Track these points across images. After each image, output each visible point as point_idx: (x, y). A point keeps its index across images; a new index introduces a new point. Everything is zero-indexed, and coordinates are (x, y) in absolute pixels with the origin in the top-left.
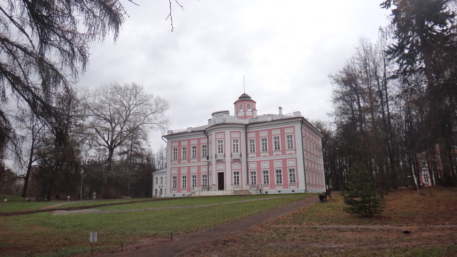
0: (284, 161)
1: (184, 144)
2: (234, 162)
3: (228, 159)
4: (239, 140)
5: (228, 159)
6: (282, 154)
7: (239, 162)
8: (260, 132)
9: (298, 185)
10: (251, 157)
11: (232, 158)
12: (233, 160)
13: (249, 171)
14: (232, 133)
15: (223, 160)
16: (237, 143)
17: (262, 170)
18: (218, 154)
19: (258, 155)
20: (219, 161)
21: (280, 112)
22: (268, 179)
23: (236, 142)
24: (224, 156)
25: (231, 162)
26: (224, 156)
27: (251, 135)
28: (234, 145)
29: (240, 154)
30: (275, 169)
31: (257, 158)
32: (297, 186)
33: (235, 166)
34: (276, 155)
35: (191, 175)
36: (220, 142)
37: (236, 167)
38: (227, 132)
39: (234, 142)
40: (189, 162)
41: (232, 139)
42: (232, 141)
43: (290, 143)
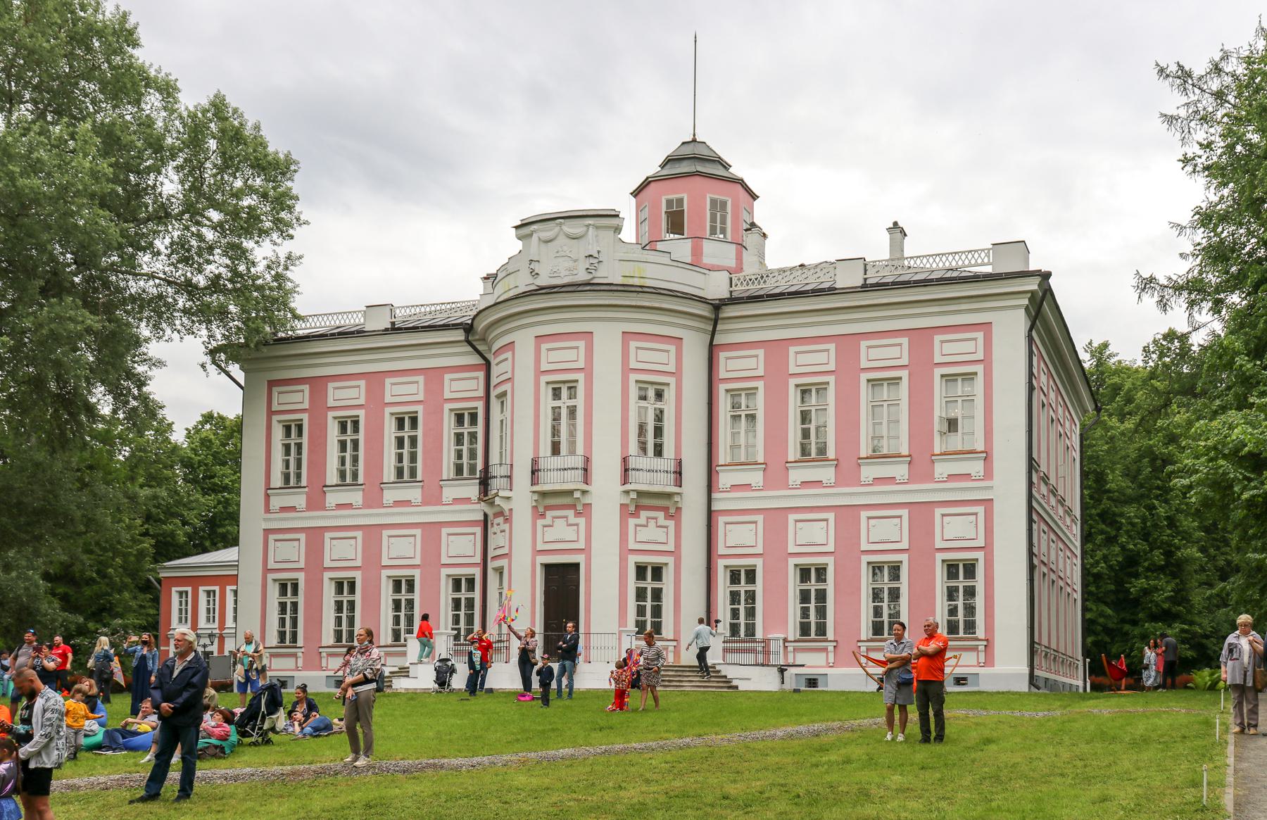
4: (673, 386)
7: (665, 509)
10: (735, 487)
11: (628, 487)
12: (633, 495)
13: (721, 563)
15: (577, 495)
18: (548, 462)
19: (775, 472)
23: (651, 393)
24: (580, 472)
26: (586, 470)
33: (644, 534)
34: (878, 480)
36: (565, 393)
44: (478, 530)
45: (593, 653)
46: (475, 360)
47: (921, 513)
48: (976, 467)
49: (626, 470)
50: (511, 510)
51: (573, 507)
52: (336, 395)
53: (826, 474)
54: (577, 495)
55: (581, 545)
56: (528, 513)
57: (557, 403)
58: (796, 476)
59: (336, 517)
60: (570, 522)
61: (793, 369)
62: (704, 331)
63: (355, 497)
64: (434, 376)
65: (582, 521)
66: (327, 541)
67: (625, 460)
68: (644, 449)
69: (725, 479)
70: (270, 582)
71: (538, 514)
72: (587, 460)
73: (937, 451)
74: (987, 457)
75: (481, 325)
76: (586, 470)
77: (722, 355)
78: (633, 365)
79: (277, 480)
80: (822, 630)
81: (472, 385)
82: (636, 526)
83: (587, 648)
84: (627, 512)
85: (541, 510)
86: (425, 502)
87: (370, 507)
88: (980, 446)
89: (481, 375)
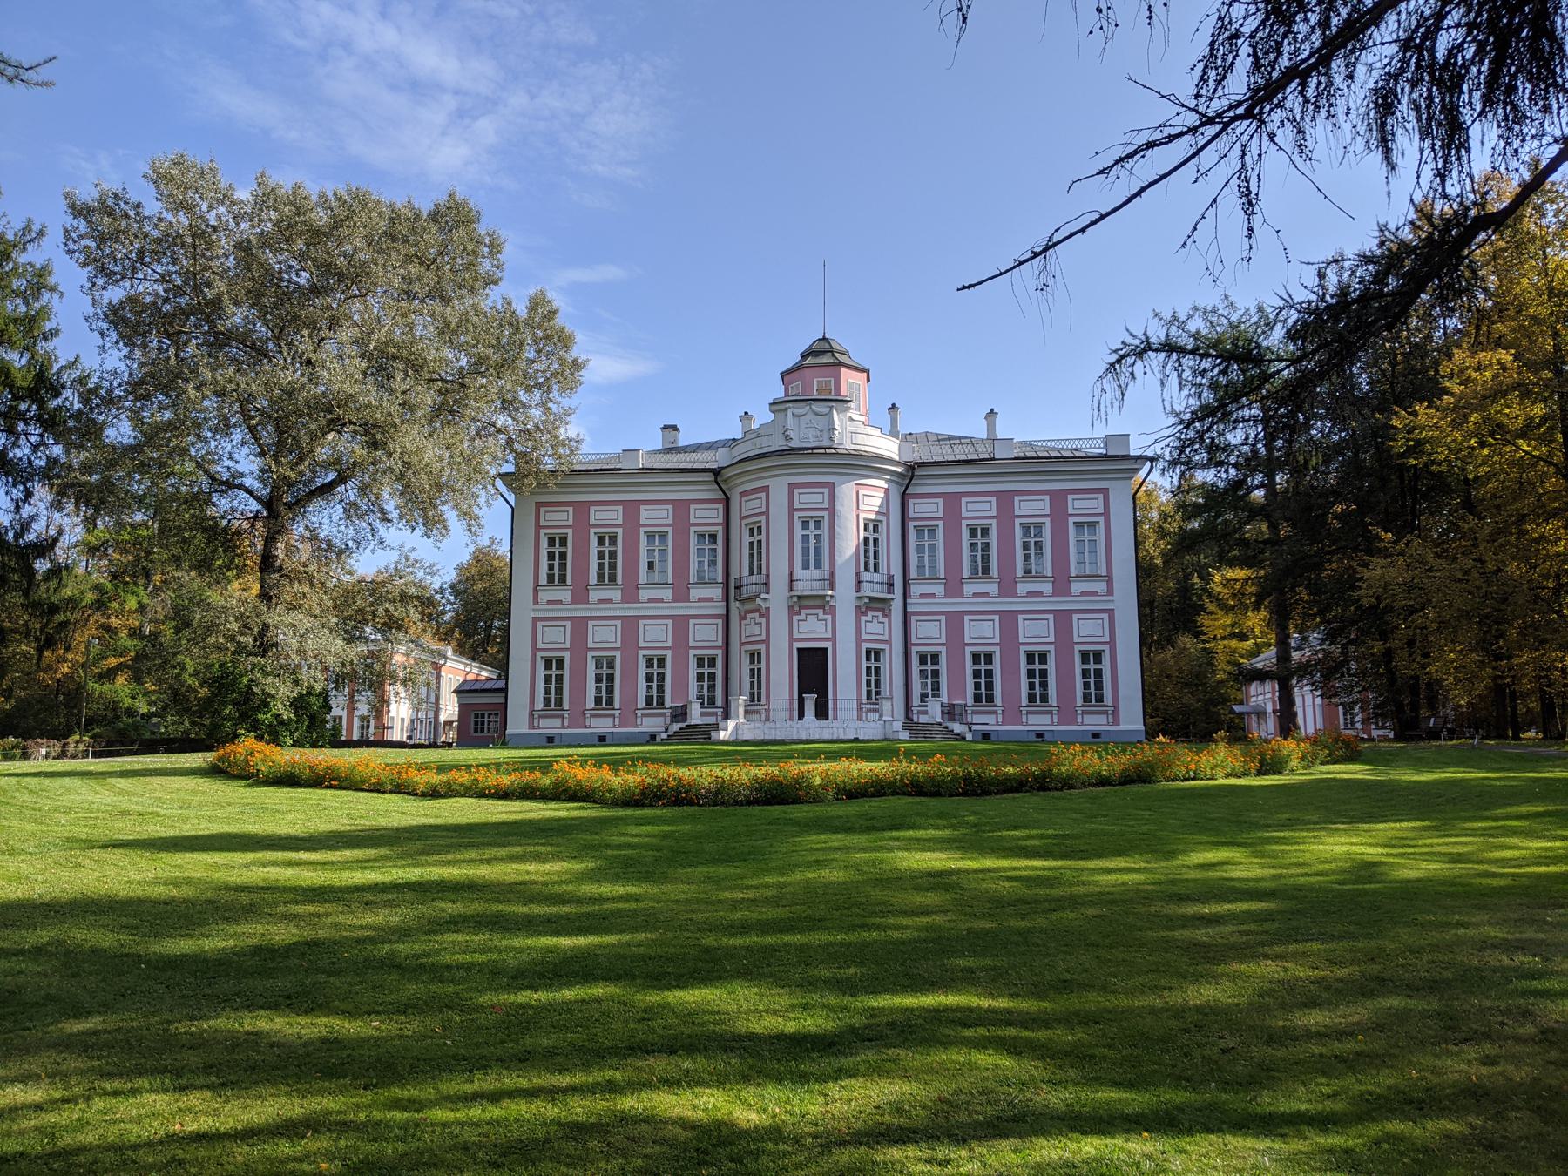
0: (1063, 620)
1: (607, 518)
2: (868, 608)
5: (845, 597)
6: (1003, 593)
8: (964, 500)
9: (1115, 707)
10: (922, 596)
13: (914, 650)
15: (828, 599)
16: (876, 536)
17: (968, 649)
18: (800, 574)
20: (801, 603)
21: (991, 427)
22: (990, 686)
25: (858, 608)
27: (926, 509)
30: (1077, 648)
32: (1111, 717)
35: (641, 653)
36: (812, 525)
37: (875, 627)
38: (779, 487)
40: (1008, 588)
43: (606, 562)
44: (720, 622)
45: (839, 713)
46: (720, 495)
50: (767, 609)
51: (823, 607)
52: (597, 516)
53: (993, 588)
54: (828, 599)
57: (806, 532)
58: (1023, 588)
62: (901, 485)
63: (615, 594)
64: (681, 507)
65: (829, 617)
66: (590, 627)
67: (858, 574)
69: (916, 589)
70: (538, 658)
72: (832, 574)
74: (1109, 579)
75: (727, 473)
77: (911, 502)
79: (543, 580)
80: (990, 698)
81: (714, 514)
83: (835, 709)
84: (860, 612)
85: (797, 608)
89: (721, 507)
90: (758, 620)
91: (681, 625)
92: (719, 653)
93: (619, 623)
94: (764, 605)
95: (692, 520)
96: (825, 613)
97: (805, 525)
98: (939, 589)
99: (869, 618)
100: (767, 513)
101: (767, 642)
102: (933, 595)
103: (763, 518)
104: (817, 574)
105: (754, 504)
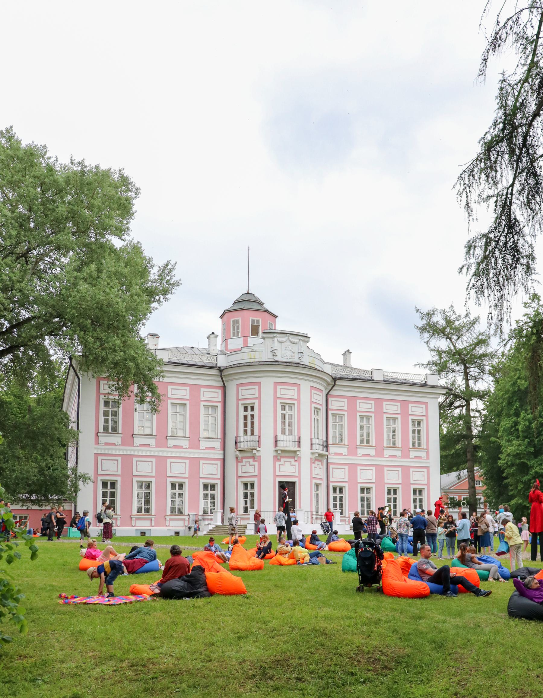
3: (305, 452)
14: (279, 387)
26: (258, 441)
28: (245, 417)
29: (257, 439)
31: (347, 457)
39: (246, 409)
41: (279, 401)
42: (279, 407)
47: (406, 470)
48: (423, 454)
49: (276, 441)
53: (372, 452)
55: (256, 474)
56: (272, 459)
59: (140, 450)
60: (251, 464)
61: (358, 409)
68: (246, 432)
71: (277, 458)
73: (385, 445)
76: (258, 441)
78: (279, 396)
82: (280, 465)
86: (190, 448)
87: (160, 447)
88: (425, 448)
90: (252, 463)
91: (194, 462)
92: (219, 483)
93: (346, 467)
94: (258, 454)
95: (202, 398)
96: (295, 461)
97: (283, 408)
98: (344, 451)
99: (316, 465)
100: (259, 398)
101: (259, 476)
102: (181, 447)
103: (256, 401)
104: (291, 438)
105: (248, 393)
